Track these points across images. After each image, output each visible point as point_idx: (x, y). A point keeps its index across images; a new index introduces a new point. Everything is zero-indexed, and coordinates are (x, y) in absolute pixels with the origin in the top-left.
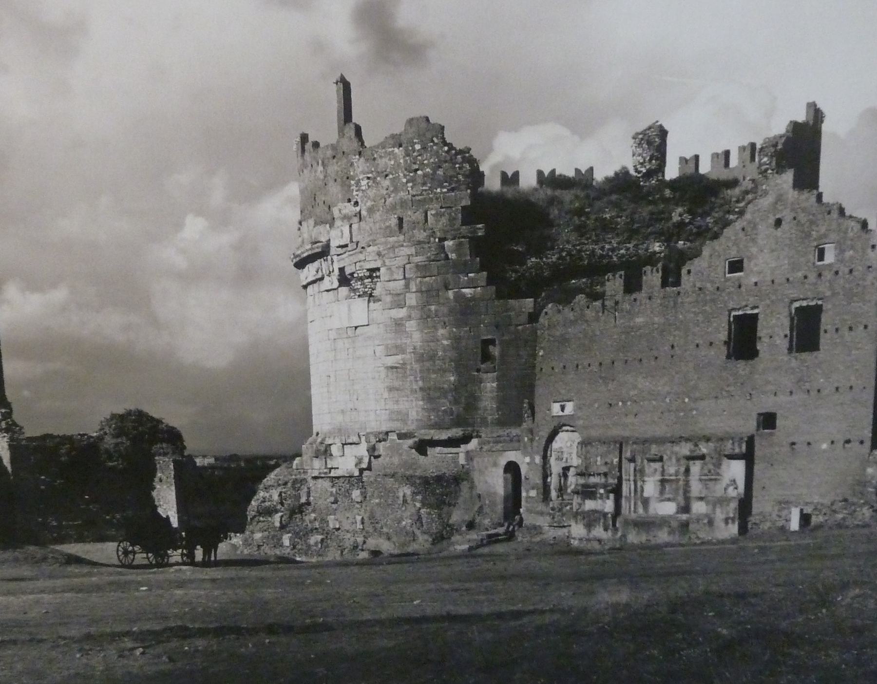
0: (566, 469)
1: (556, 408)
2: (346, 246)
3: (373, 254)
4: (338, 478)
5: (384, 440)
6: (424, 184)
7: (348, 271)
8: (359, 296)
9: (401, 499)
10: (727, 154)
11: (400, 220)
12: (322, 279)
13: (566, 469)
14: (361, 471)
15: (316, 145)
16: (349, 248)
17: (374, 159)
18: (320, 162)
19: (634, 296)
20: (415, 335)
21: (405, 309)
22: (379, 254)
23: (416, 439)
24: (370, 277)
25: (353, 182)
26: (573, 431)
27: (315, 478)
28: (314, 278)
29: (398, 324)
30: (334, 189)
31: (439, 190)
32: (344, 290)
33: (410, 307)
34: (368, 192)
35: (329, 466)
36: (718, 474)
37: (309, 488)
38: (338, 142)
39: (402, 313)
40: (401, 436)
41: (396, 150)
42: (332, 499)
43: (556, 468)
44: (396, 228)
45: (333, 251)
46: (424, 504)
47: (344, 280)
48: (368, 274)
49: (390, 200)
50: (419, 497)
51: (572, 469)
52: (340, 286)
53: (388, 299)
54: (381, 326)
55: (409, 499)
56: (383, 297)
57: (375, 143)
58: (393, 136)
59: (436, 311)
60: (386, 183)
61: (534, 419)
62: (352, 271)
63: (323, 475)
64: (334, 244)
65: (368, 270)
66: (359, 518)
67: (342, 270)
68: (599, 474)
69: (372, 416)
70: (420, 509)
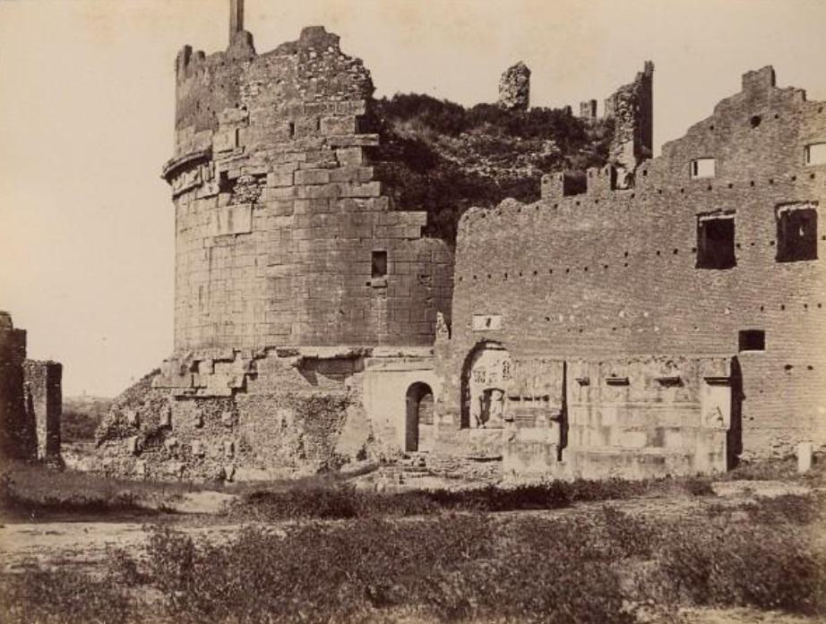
0: (489, 392)
1: (479, 323)
2: (231, 150)
3: (261, 160)
4: (205, 399)
5: (263, 357)
6: (318, 92)
7: (231, 175)
8: (242, 202)
9: (280, 423)
10: (594, 103)
11: (292, 125)
12: (200, 186)
13: (489, 392)
14: (235, 390)
15: (202, 54)
16: (234, 153)
17: (267, 66)
18: (207, 69)
19: (576, 199)
20: (302, 245)
21: (292, 217)
22: (267, 160)
23: (300, 357)
24: (256, 182)
25: (242, 88)
26: (498, 349)
27: (179, 398)
28: (191, 185)
29: (284, 232)
30: (220, 95)
31: (332, 98)
32: (225, 197)
33: (298, 215)
34: (258, 97)
35: (196, 385)
36: (696, 401)
37: (170, 409)
38: (228, 50)
39: (290, 221)
40: (284, 354)
41: (290, 57)
42: (198, 422)
43: (476, 391)
44: (288, 134)
45: (215, 156)
46: (307, 431)
47: (228, 184)
48: (252, 179)
49: (281, 106)
50: (302, 422)
51: (494, 393)
52: (221, 191)
53: (275, 205)
54: (265, 233)
55: (290, 422)
56: (268, 204)
57: (269, 49)
58: (287, 44)
59: (326, 219)
60: (278, 89)
61: (450, 334)
62: (236, 176)
63: (188, 395)
64: (216, 149)
65: (254, 176)
66: (228, 444)
67: (224, 175)
68: (538, 399)
69: (250, 330)
70: (301, 436)
